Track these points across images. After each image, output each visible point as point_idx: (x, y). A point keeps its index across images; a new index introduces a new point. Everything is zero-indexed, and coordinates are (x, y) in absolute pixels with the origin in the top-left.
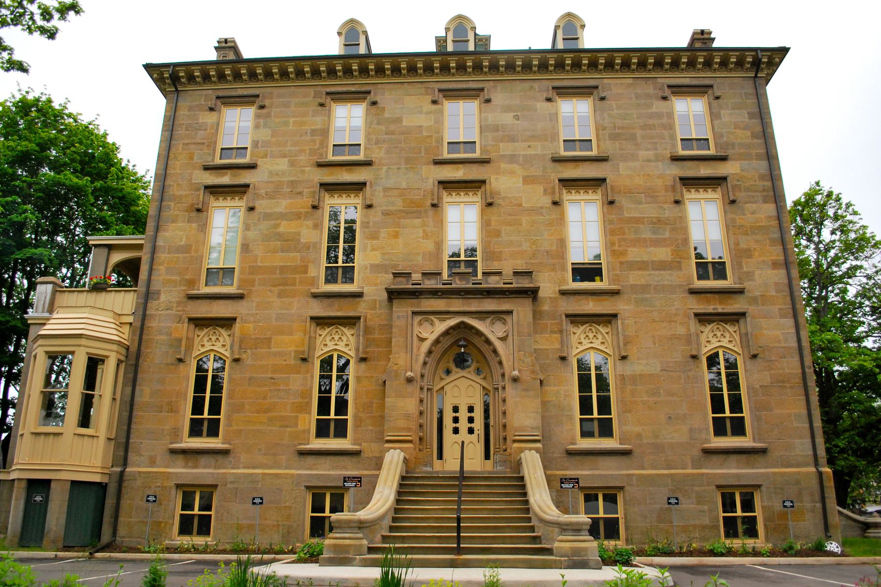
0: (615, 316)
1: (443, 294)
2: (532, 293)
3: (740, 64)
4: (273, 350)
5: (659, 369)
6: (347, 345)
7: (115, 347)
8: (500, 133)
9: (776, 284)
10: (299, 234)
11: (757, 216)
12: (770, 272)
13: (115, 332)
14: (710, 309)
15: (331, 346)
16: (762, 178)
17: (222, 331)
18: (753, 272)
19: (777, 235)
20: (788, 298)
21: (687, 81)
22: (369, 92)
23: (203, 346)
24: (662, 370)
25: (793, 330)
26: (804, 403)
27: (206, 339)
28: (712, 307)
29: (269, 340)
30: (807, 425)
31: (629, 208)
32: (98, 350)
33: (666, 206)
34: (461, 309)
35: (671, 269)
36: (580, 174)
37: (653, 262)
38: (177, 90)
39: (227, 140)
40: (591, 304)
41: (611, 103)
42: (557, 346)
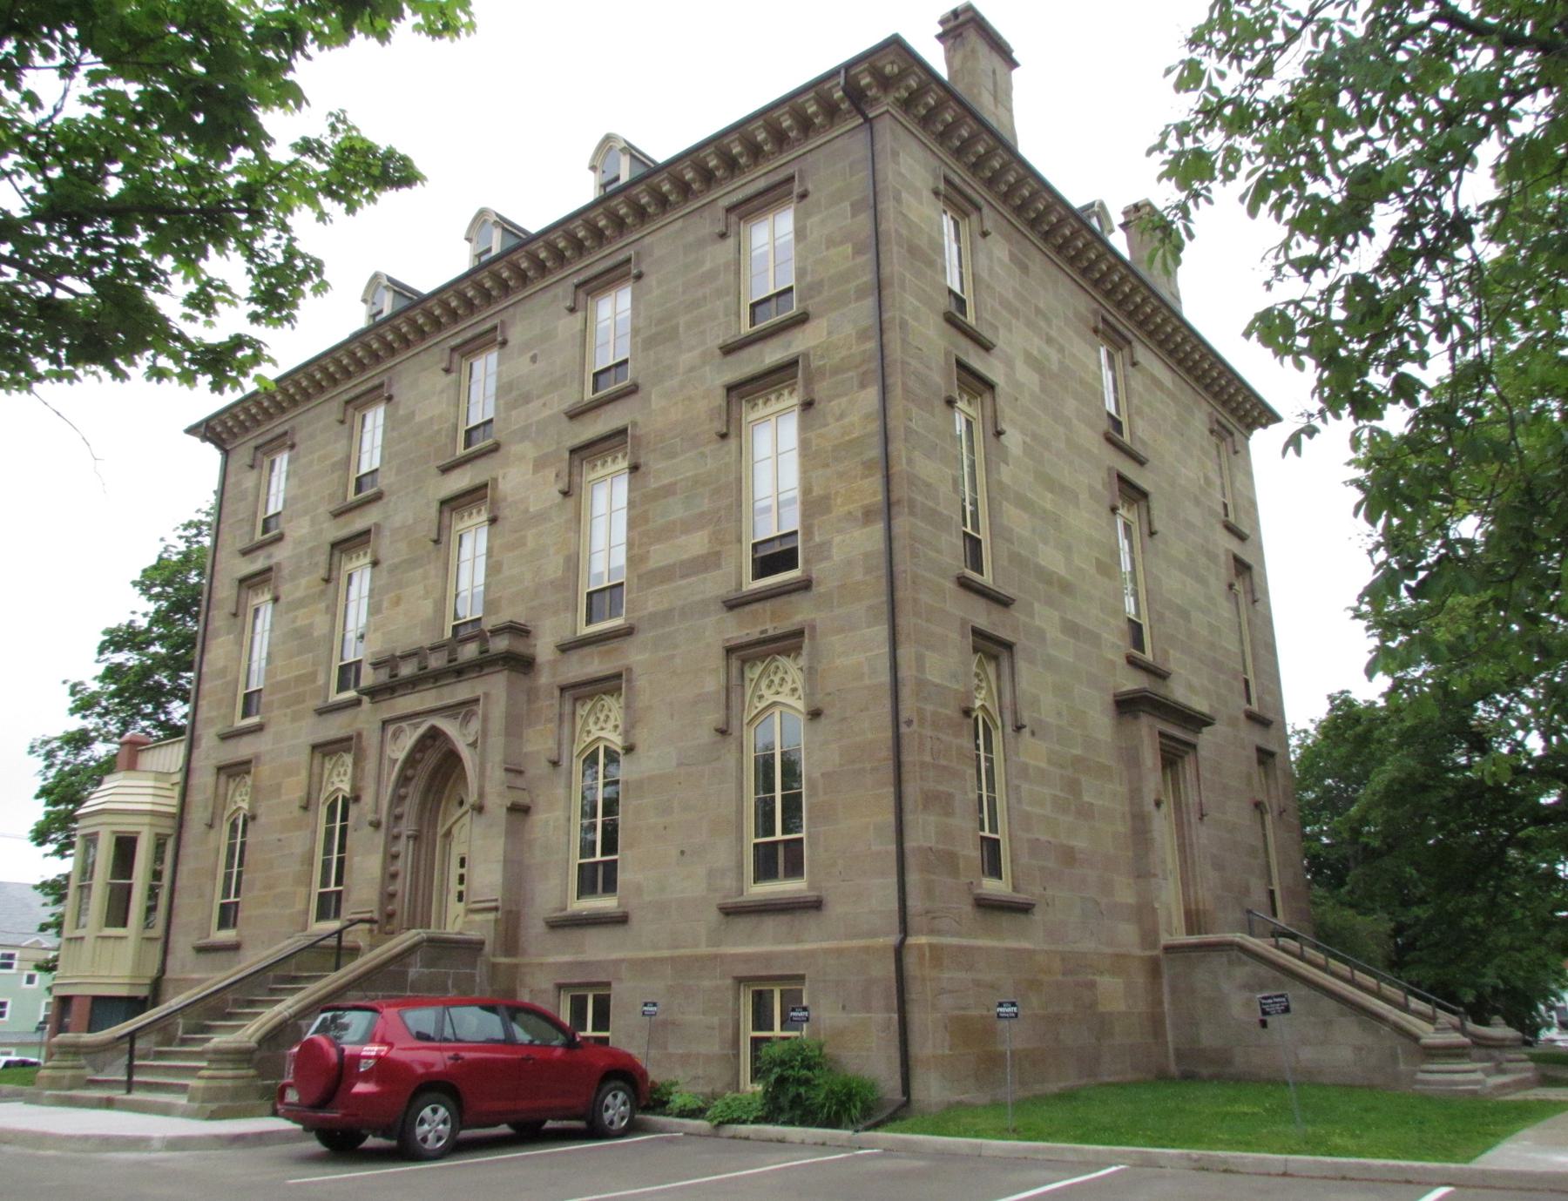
0: (799, 633)
1: (436, 680)
2: (521, 664)
3: (832, 112)
4: (284, 798)
5: (674, 763)
6: (794, 690)
7: (147, 819)
8: (515, 393)
9: (866, 555)
10: (311, 625)
11: (846, 421)
12: (857, 533)
13: (150, 799)
14: (753, 632)
15: (596, 733)
16: (862, 336)
17: (783, 661)
18: (830, 542)
19: (875, 452)
20: (884, 582)
21: (761, 184)
22: (791, 179)
23: (761, 697)
24: (680, 765)
25: (886, 649)
26: (890, 801)
27: (591, 720)
28: (759, 628)
29: (279, 786)
30: (893, 848)
31: (660, 471)
32: (126, 826)
33: (707, 450)
34: (439, 704)
35: (706, 569)
36: (601, 430)
37: (682, 563)
38: (867, 120)
39: (763, 284)
40: (596, 661)
41: (651, 280)
42: (551, 743)
